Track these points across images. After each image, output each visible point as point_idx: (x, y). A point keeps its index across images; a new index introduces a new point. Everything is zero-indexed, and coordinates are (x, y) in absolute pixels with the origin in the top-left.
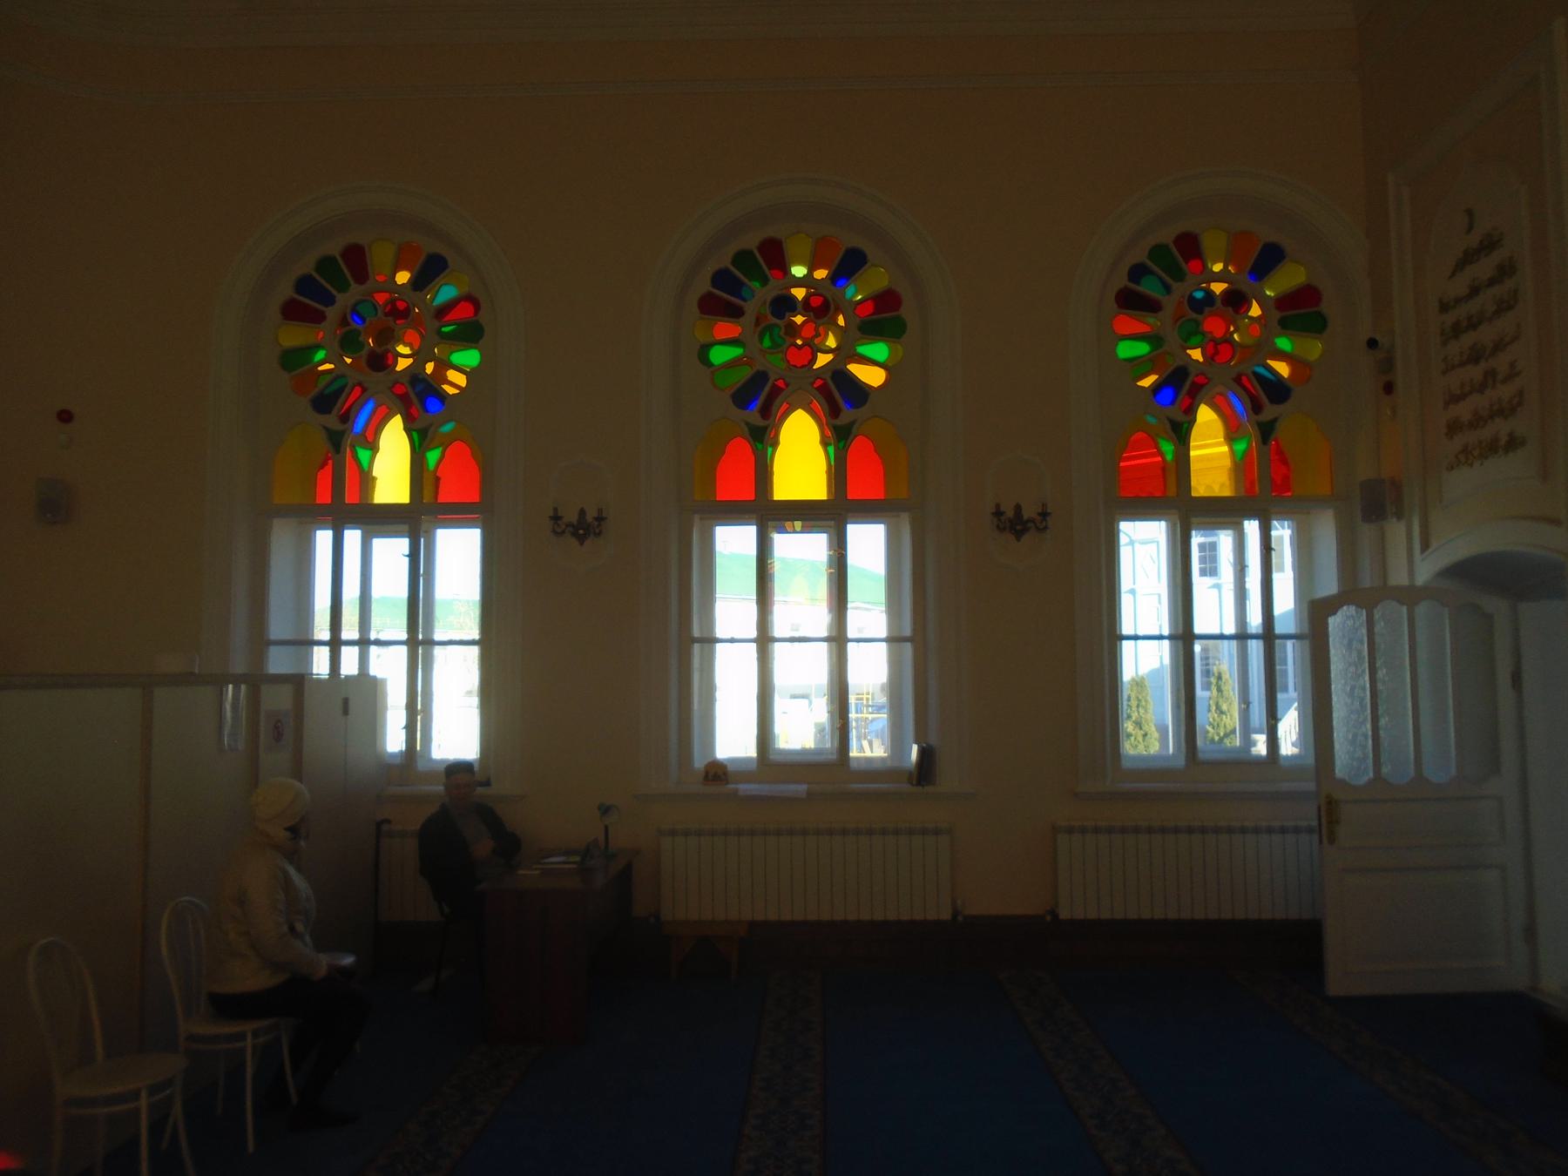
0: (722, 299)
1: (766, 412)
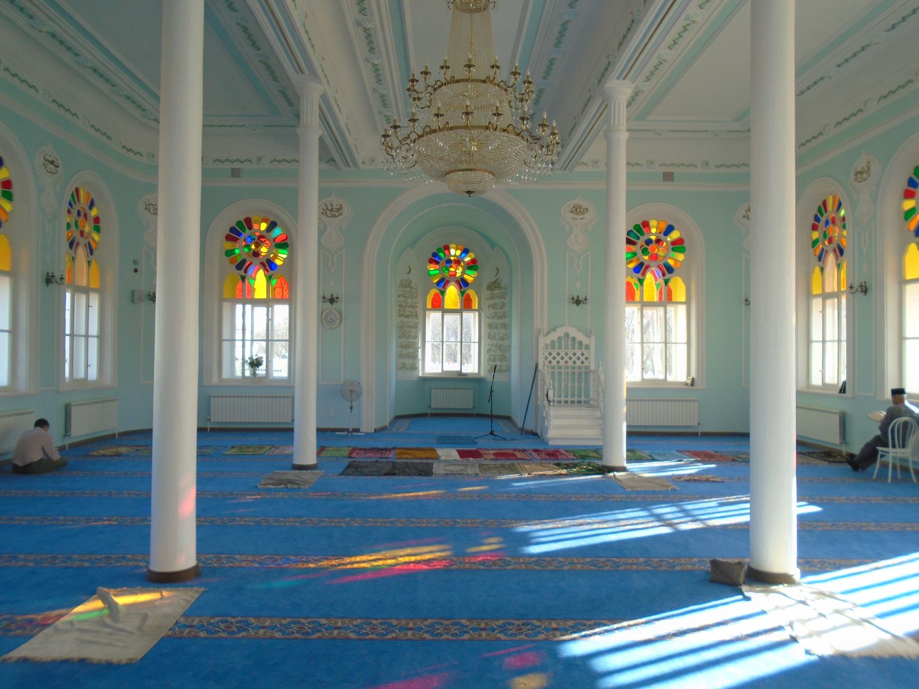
0: (434, 260)
1: (445, 287)
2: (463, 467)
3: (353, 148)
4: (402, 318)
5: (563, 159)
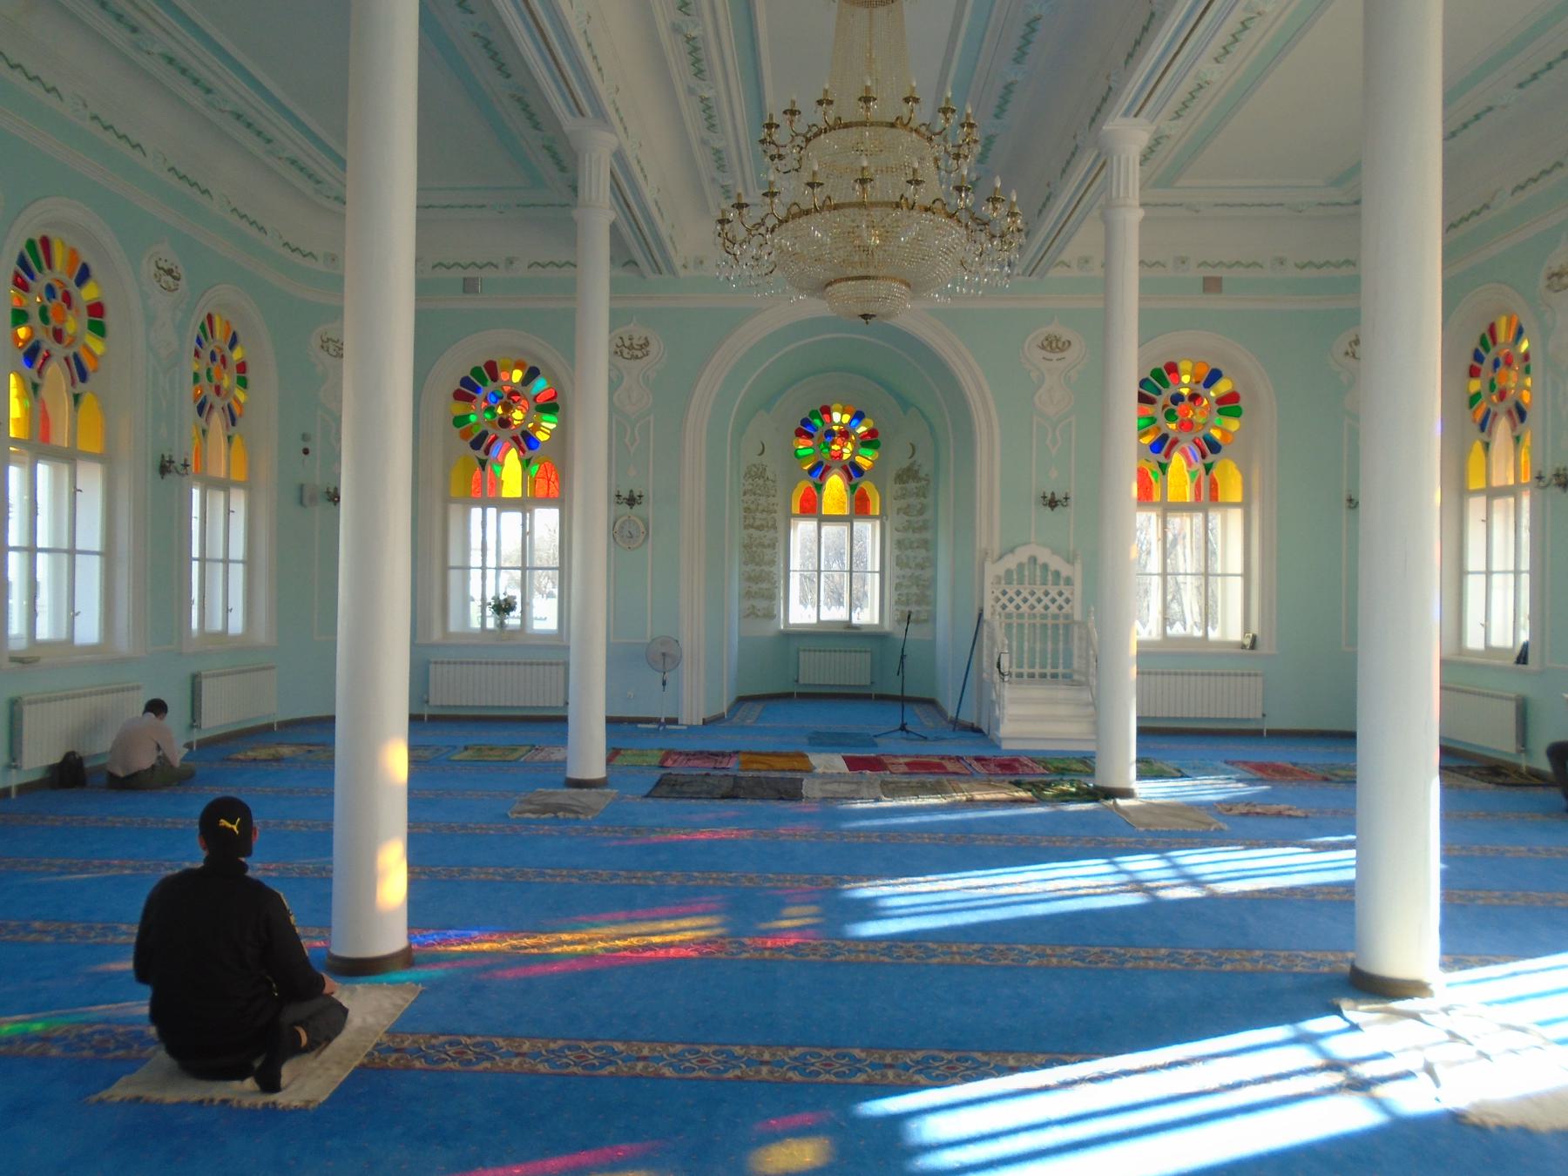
0: (805, 430)
1: (823, 477)
2: (854, 787)
3: (667, 241)
4: (752, 531)
5: (1030, 254)
